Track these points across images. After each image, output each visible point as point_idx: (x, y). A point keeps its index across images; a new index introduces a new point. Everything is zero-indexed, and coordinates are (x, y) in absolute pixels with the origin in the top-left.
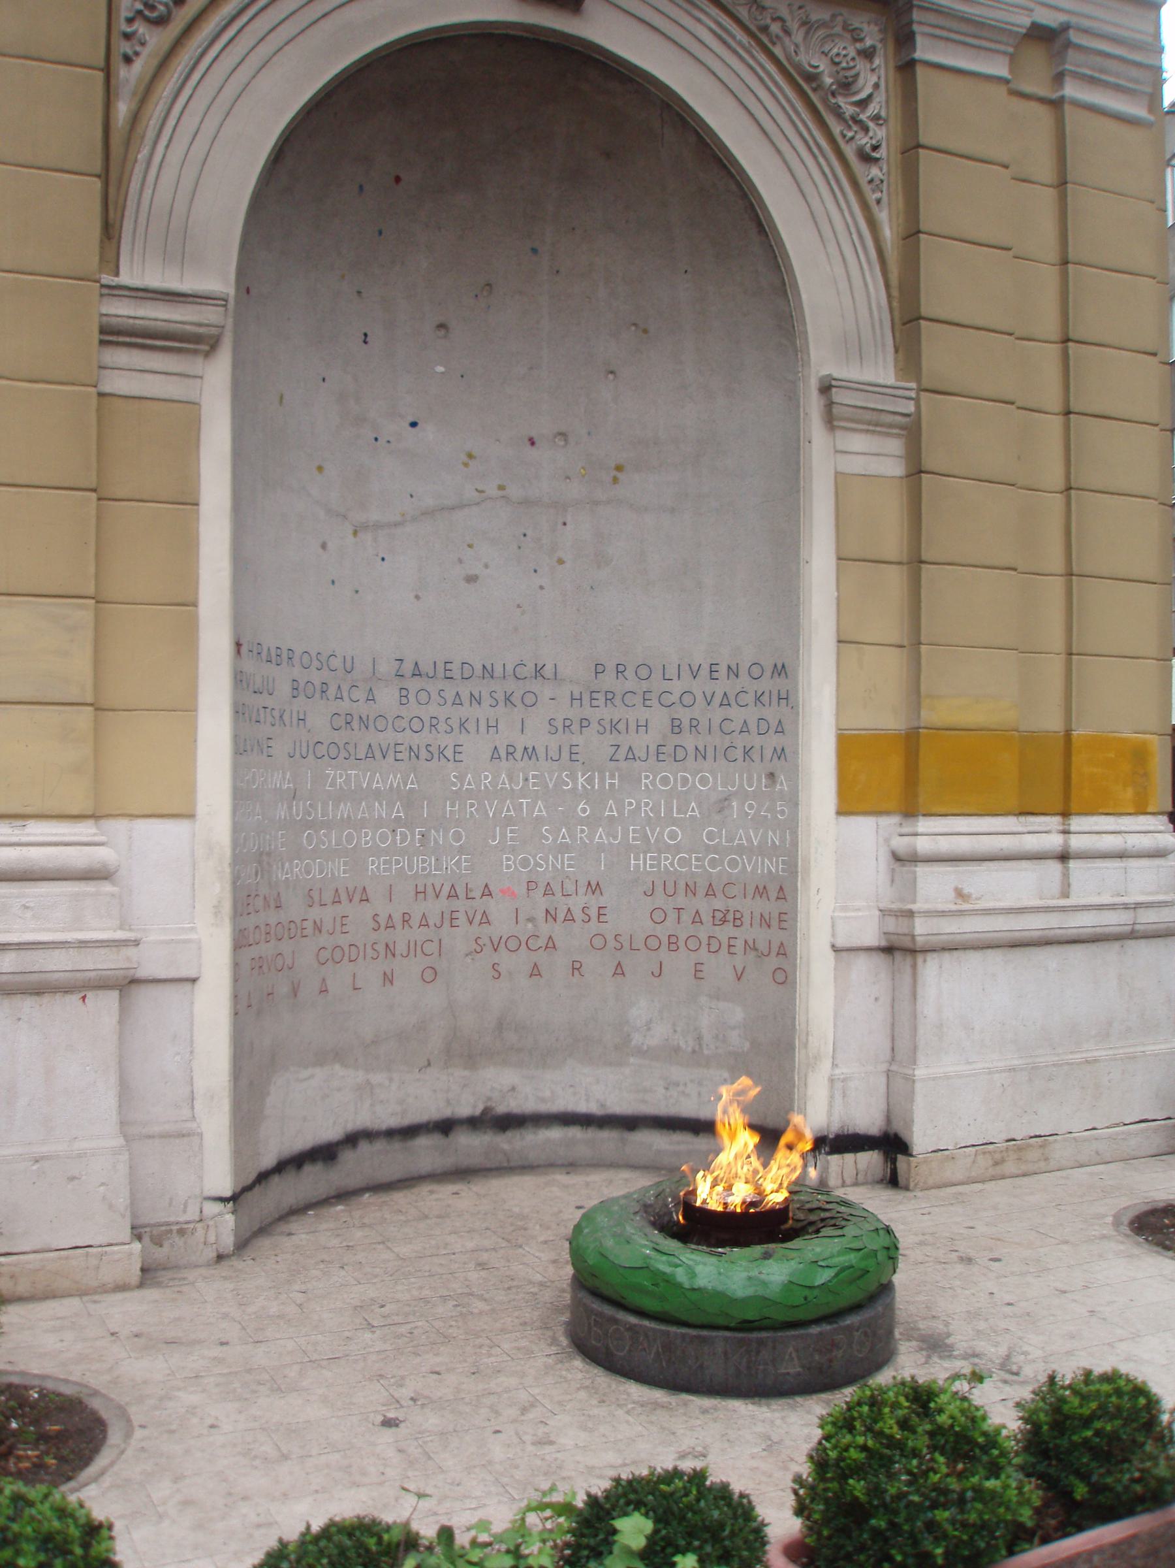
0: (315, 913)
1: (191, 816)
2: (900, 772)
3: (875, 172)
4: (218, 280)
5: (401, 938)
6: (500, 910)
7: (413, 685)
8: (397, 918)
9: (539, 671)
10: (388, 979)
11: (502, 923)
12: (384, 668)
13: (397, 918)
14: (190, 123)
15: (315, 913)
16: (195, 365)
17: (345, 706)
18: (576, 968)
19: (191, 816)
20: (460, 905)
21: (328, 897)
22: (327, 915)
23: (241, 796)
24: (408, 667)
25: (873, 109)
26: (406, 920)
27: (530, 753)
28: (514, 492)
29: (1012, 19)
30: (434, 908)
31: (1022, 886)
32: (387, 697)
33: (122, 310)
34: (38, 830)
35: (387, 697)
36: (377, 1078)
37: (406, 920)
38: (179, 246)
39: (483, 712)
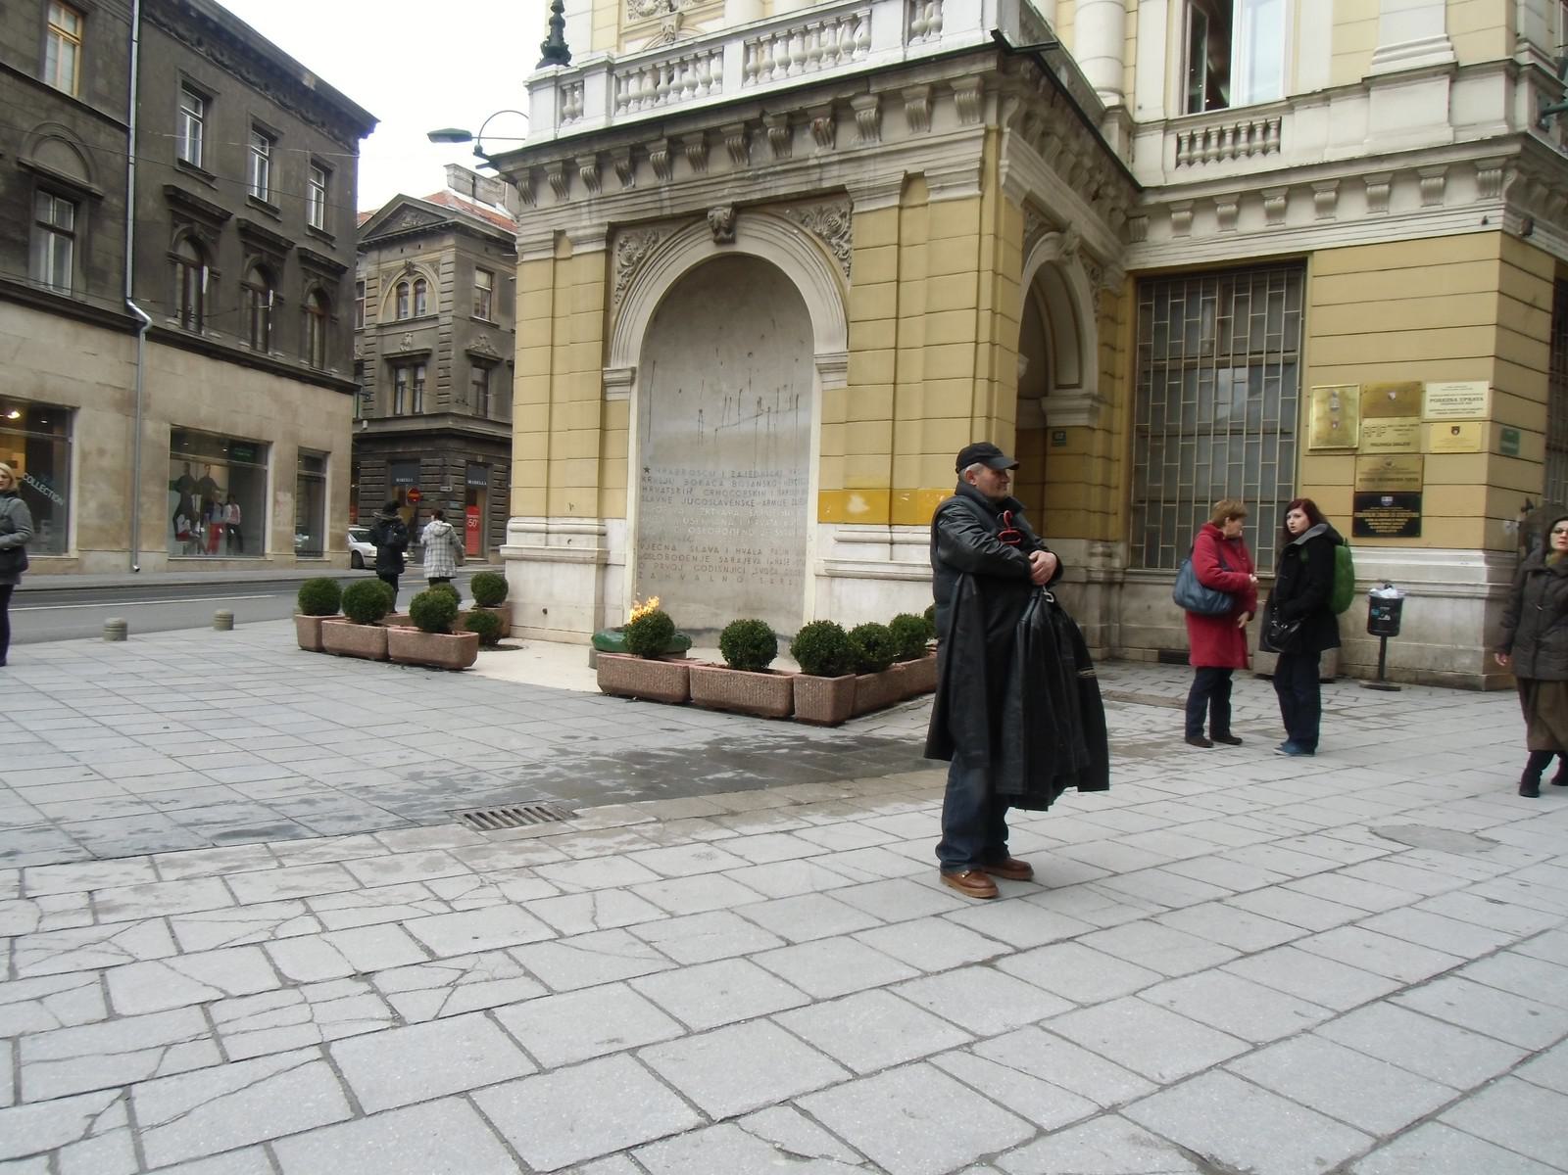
0: (694, 554)
1: (625, 519)
2: (834, 508)
3: (846, 265)
4: (635, 363)
5: (730, 565)
6: (763, 560)
7: (737, 480)
8: (729, 559)
9: (777, 474)
10: (725, 579)
11: (764, 564)
12: (728, 475)
13: (729, 559)
14: (629, 317)
15: (694, 554)
16: (628, 389)
17: (711, 487)
18: (782, 581)
19: (625, 519)
20: (751, 556)
21: (700, 548)
22: (700, 556)
23: (641, 514)
24: (736, 475)
25: (846, 237)
26: (733, 560)
27: (774, 503)
28: (774, 409)
29: (895, 179)
30: (743, 556)
31: (879, 553)
32: (727, 485)
33: (607, 377)
34: (586, 521)
35: (727, 485)
36: (719, 612)
37: (733, 560)
38: (625, 358)
39: (761, 489)
